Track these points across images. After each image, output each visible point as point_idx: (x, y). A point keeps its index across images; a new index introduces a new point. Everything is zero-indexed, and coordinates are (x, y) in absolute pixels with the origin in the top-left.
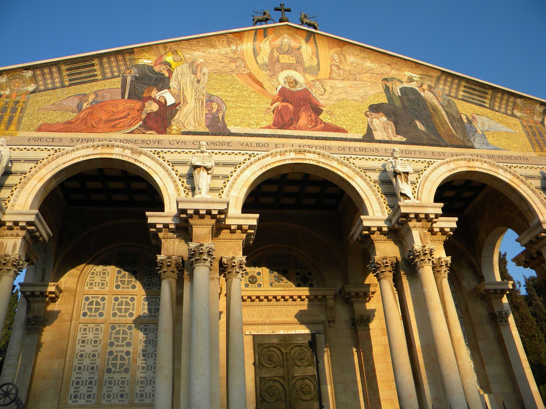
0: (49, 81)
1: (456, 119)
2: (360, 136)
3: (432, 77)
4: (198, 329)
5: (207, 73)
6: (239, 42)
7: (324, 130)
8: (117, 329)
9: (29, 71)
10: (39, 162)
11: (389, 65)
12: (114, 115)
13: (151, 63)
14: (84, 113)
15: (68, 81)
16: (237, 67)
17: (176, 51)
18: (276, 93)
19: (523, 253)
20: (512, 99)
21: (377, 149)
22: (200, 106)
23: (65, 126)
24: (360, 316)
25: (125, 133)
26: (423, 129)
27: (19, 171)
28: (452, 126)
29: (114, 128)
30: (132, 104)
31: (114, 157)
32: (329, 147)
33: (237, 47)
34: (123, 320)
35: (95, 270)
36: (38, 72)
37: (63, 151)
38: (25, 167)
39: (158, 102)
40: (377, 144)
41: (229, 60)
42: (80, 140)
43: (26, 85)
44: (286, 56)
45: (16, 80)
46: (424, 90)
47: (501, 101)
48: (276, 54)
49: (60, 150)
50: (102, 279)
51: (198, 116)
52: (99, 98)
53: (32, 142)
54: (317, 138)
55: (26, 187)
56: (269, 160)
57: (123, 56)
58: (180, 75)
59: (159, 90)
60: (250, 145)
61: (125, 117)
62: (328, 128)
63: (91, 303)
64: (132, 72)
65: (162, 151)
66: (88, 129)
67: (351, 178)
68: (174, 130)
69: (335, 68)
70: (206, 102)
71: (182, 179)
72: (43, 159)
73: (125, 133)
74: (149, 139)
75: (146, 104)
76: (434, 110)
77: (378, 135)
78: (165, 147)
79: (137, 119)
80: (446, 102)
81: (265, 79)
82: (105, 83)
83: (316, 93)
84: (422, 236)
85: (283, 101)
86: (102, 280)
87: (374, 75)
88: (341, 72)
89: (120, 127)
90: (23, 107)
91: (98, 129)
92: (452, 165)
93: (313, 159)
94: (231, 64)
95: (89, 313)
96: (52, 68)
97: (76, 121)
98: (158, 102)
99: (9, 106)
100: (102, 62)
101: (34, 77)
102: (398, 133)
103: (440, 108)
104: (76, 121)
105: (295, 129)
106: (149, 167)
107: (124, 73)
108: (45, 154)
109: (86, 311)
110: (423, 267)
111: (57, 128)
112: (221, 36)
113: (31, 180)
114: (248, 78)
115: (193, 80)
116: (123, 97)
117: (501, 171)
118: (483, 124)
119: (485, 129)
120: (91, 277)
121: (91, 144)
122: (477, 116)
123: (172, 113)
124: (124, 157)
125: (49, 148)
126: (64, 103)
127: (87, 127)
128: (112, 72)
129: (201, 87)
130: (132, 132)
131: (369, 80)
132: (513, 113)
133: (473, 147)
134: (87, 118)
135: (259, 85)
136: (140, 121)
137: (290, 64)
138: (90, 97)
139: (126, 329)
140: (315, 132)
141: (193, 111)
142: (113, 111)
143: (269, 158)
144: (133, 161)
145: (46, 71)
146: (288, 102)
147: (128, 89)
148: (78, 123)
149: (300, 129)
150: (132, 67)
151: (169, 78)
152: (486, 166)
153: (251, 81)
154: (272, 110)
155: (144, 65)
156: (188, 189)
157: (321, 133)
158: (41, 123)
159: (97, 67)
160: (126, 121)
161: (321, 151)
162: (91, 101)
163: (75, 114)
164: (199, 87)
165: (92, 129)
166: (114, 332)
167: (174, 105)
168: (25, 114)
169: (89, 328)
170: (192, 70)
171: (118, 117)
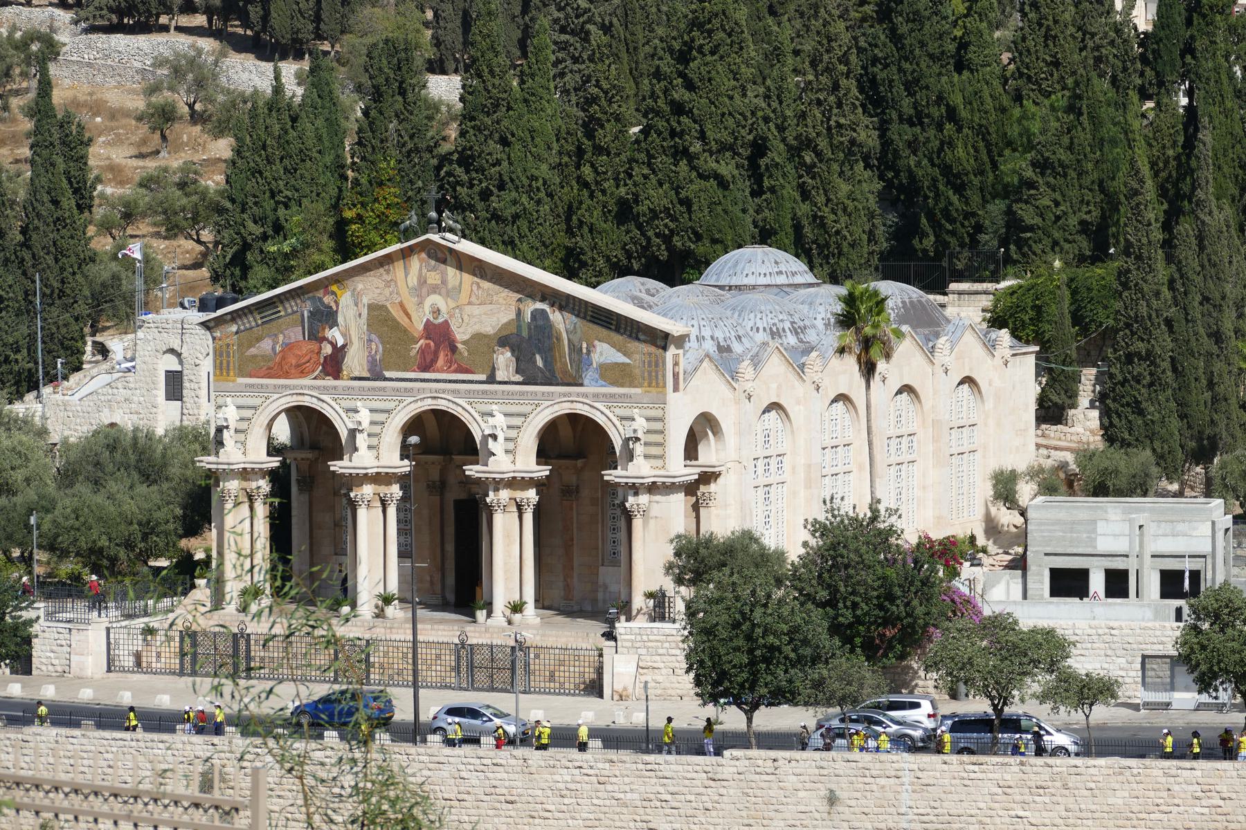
1: (575, 349)
2: (483, 377)
7: (456, 371)
18: (421, 327)
29: (303, 374)
39: (331, 343)
44: (433, 273)
48: (424, 271)
54: (450, 381)
56: (413, 406)
69: (475, 287)
77: (500, 376)
92: (556, 407)
98: (331, 343)
102: (517, 372)
103: (564, 335)
117: (598, 414)
118: (601, 354)
119: (602, 360)
122: (596, 343)
133: (582, 385)
151: (336, 312)
152: (587, 408)
153: (402, 313)
165: (287, 375)
167: (344, 346)
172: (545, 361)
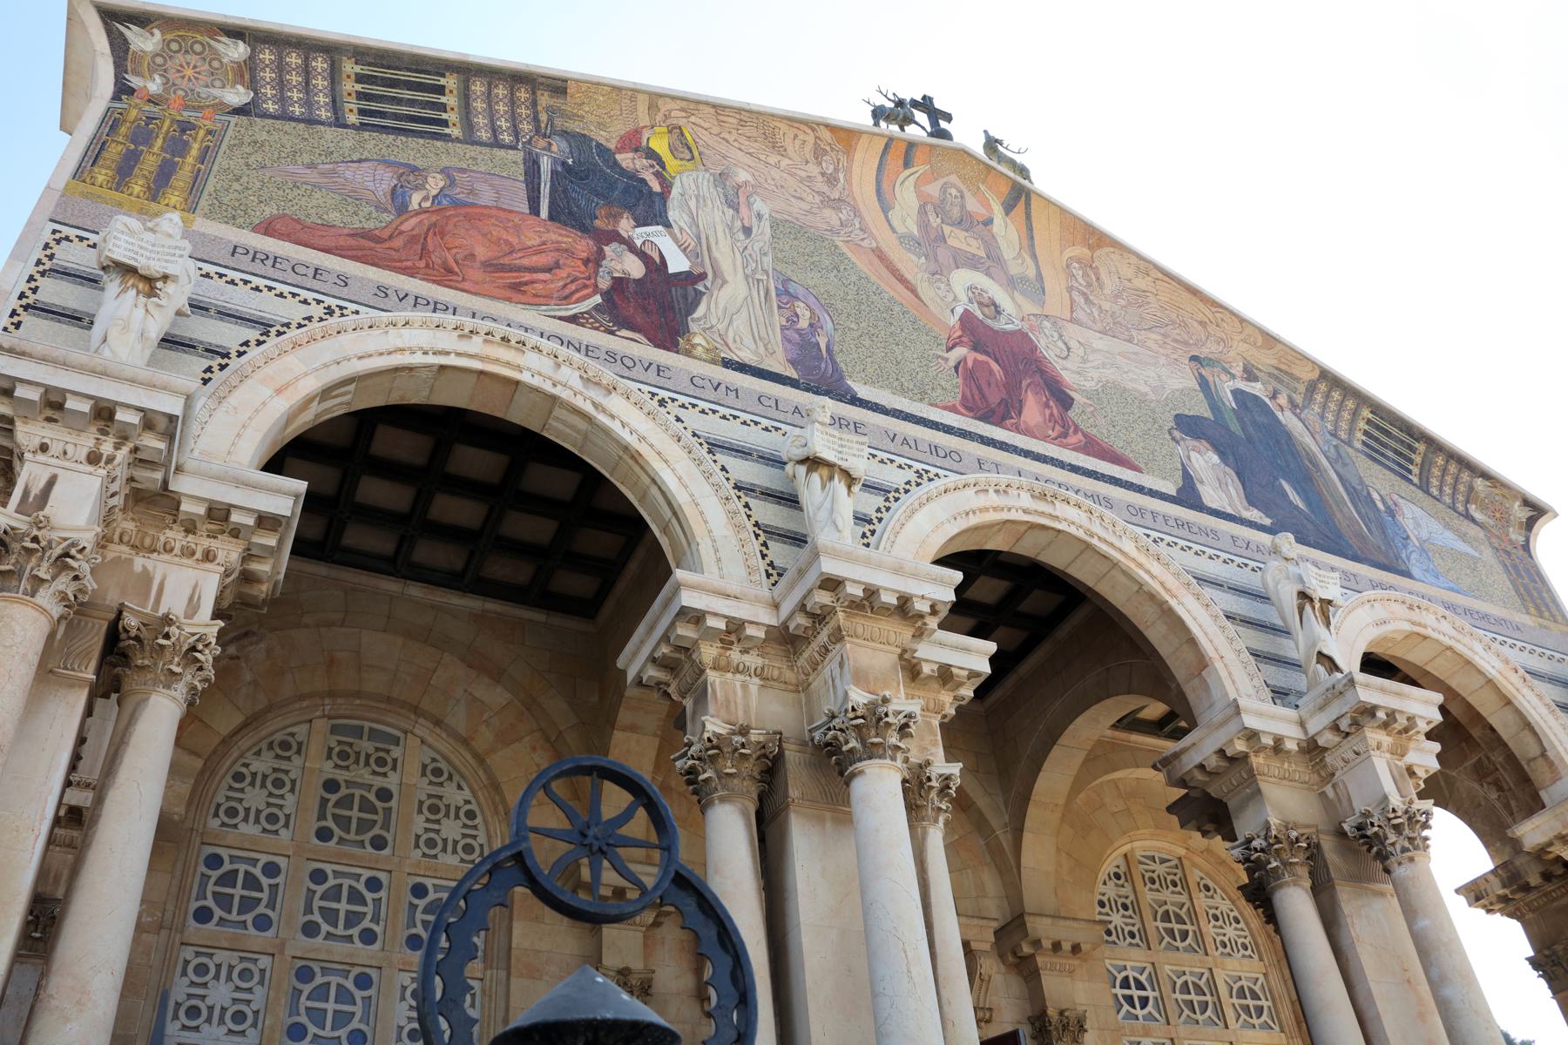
0: (295, 95)
1: (1360, 496)
2: (1171, 489)
3: (1298, 379)
4: (909, 971)
5: (767, 216)
6: (843, 159)
8: (319, 980)
9: (241, 43)
10: (273, 331)
11: (1201, 323)
12: (511, 253)
13: (607, 140)
14: (413, 221)
15: (356, 111)
16: (842, 224)
17: (680, 128)
18: (953, 320)
19: (1492, 872)
20: (1465, 476)
21: (1214, 532)
22: (763, 299)
23: (352, 242)
24: (1061, 1013)
25: (554, 317)
26: (1301, 505)
27: (201, 342)
28: (1359, 513)
29: (517, 291)
30: (565, 239)
31: (525, 377)
32: (1109, 503)
33: (836, 170)
34: (340, 950)
35: (246, 765)
36: (267, 56)
37: (355, 316)
38: (228, 335)
40: (1212, 519)
41: (818, 199)
42: (411, 300)
43: (218, 83)
45: (188, 57)
46: (1282, 410)
47: (1443, 476)
48: (935, 221)
49: (345, 311)
50: (272, 800)
51: (762, 328)
52: (458, 190)
53: (244, 261)
54: (1075, 469)
55: (233, 399)
56: (970, 499)
57: (534, 93)
58: (694, 199)
59: (641, 223)
60: (913, 445)
61: (549, 270)
62: (1092, 447)
63: (229, 879)
64: (554, 148)
65: (673, 400)
66: (430, 272)
67: (1173, 596)
68: (699, 348)
69: (1080, 300)
70: (777, 295)
71: (745, 499)
72: (288, 325)
73: (554, 317)
74: (628, 352)
75: (605, 248)
76: (1311, 462)
77: (1210, 495)
78: (679, 389)
79: (586, 286)
80: (1332, 450)
81: (919, 276)
82: (473, 154)
83: (1048, 347)
84: (1396, 773)
85: (975, 348)
86: (269, 805)
87: (1167, 340)
88: (1096, 314)
89: (535, 296)
90: (208, 147)
91: (464, 279)
93: (1077, 521)
94: (825, 211)
95: (218, 913)
96: (315, 59)
97: (391, 237)
99: (160, 128)
100: (467, 88)
101: (251, 66)
102: (1252, 502)
104: (391, 237)
105: (1017, 429)
106: (642, 439)
107: (529, 142)
108: (294, 311)
109: (210, 902)
110: (1411, 860)
111: (331, 243)
112: (802, 126)
113: (249, 382)
114: (876, 261)
115: (732, 222)
116: (535, 210)
120: (231, 788)
121: (448, 318)
122: (1401, 500)
123: (685, 297)
124: (559, 387)
125: (304, 294)
126: (348, 174)
127: (427, 266)
128: (495, 131)
129: (756, 249)
130: (573, 319)
131: (1161, 350)
132: (1467, 509)
133: (1407, 574)
134: (425, 238)
135: (907, 288)
136: (595, 293)
137: (974, 255)
138: (430, 179)
139: (350, 984)
140: (1067, 452)
141: (745, 309)
142: (506, 241)
143: (970, 492)
144: (588, 408)
145: (294, 59)
146: (987, 353)
147: (547, 190)
148: (398, 242)
149: (1028, 432)
150: (554, 132)
151: (664, 196)
154: (952, 363)
155: (592, 140)
156: (764, 531)
157: (1082, 456)
158: (270, 210)
159: (450, 100)
160: (556, 282)
161: (1089, 502)
162: (434, 192)
163: (387, 217)
164: (750, 247)
165: (446, 275)
166: (307, 989)
167: (690, 279)
168: (215, 168)
169: (219, 966)
170: (726, 196)
171: (526, 262)
172: (1306, 500)
